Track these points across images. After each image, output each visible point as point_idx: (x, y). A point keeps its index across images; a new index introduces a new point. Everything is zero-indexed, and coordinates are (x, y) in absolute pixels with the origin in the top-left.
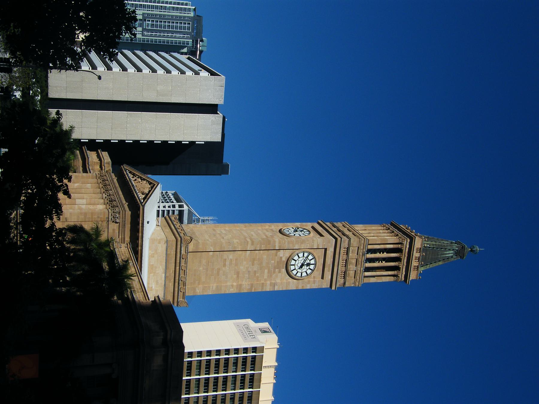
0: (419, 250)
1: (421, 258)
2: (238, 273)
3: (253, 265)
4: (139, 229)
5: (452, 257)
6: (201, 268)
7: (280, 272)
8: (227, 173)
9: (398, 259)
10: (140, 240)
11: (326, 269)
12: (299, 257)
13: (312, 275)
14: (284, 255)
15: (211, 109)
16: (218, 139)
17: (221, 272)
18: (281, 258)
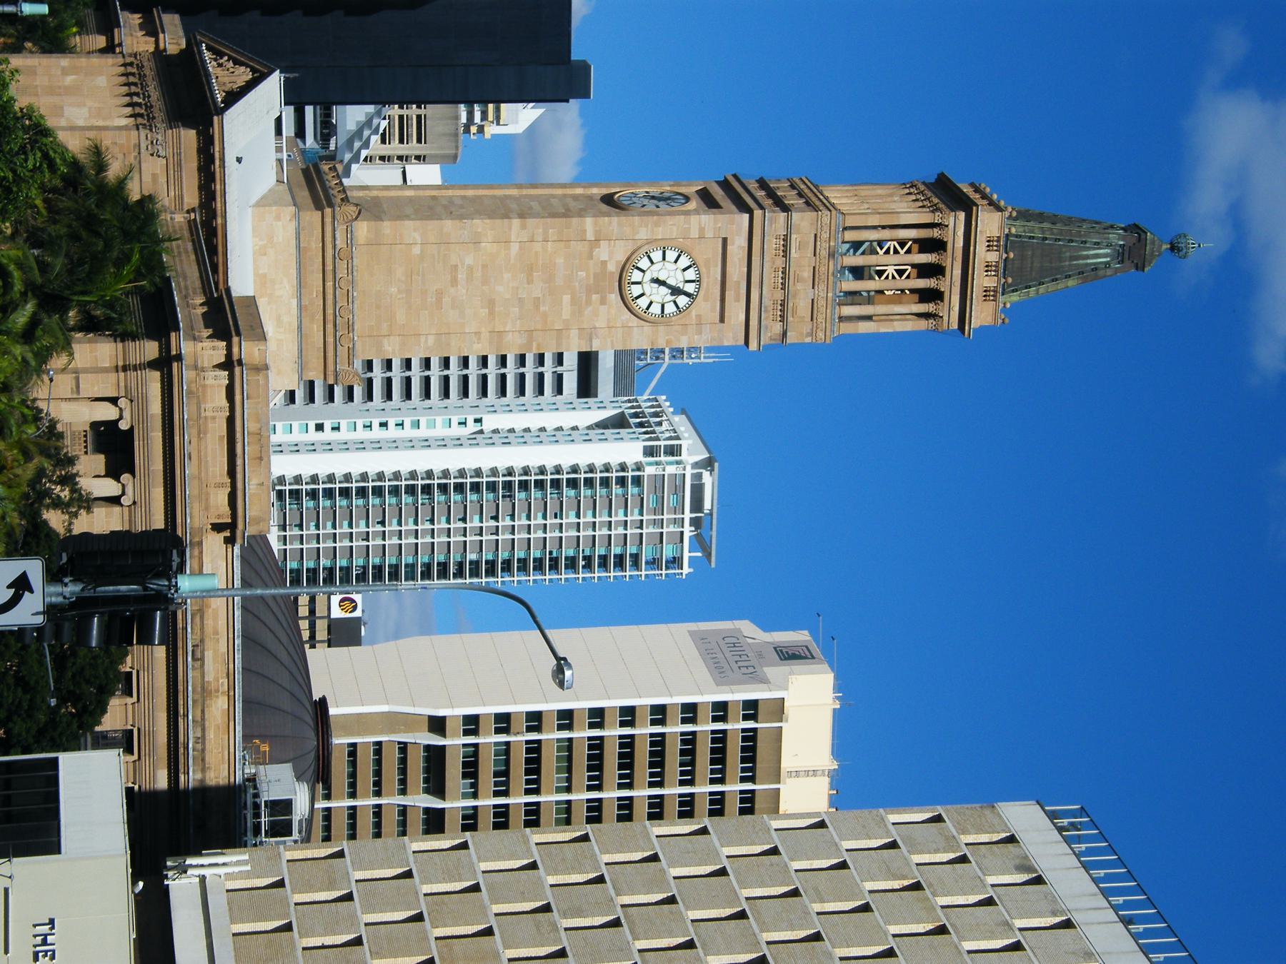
1: (1001, 265)
2: (491, 304)
3: (530, 282)
4: (214, 173)
5: (1107, 265)
6: (394, 290)
7: (603, 301)
8: (586, 94)
9: (934, 271)
10: (218, 199)
11: (729, 295)
12: (652, 262)
13: (694, 312)
17: (446, 300)
18: (604, 263)
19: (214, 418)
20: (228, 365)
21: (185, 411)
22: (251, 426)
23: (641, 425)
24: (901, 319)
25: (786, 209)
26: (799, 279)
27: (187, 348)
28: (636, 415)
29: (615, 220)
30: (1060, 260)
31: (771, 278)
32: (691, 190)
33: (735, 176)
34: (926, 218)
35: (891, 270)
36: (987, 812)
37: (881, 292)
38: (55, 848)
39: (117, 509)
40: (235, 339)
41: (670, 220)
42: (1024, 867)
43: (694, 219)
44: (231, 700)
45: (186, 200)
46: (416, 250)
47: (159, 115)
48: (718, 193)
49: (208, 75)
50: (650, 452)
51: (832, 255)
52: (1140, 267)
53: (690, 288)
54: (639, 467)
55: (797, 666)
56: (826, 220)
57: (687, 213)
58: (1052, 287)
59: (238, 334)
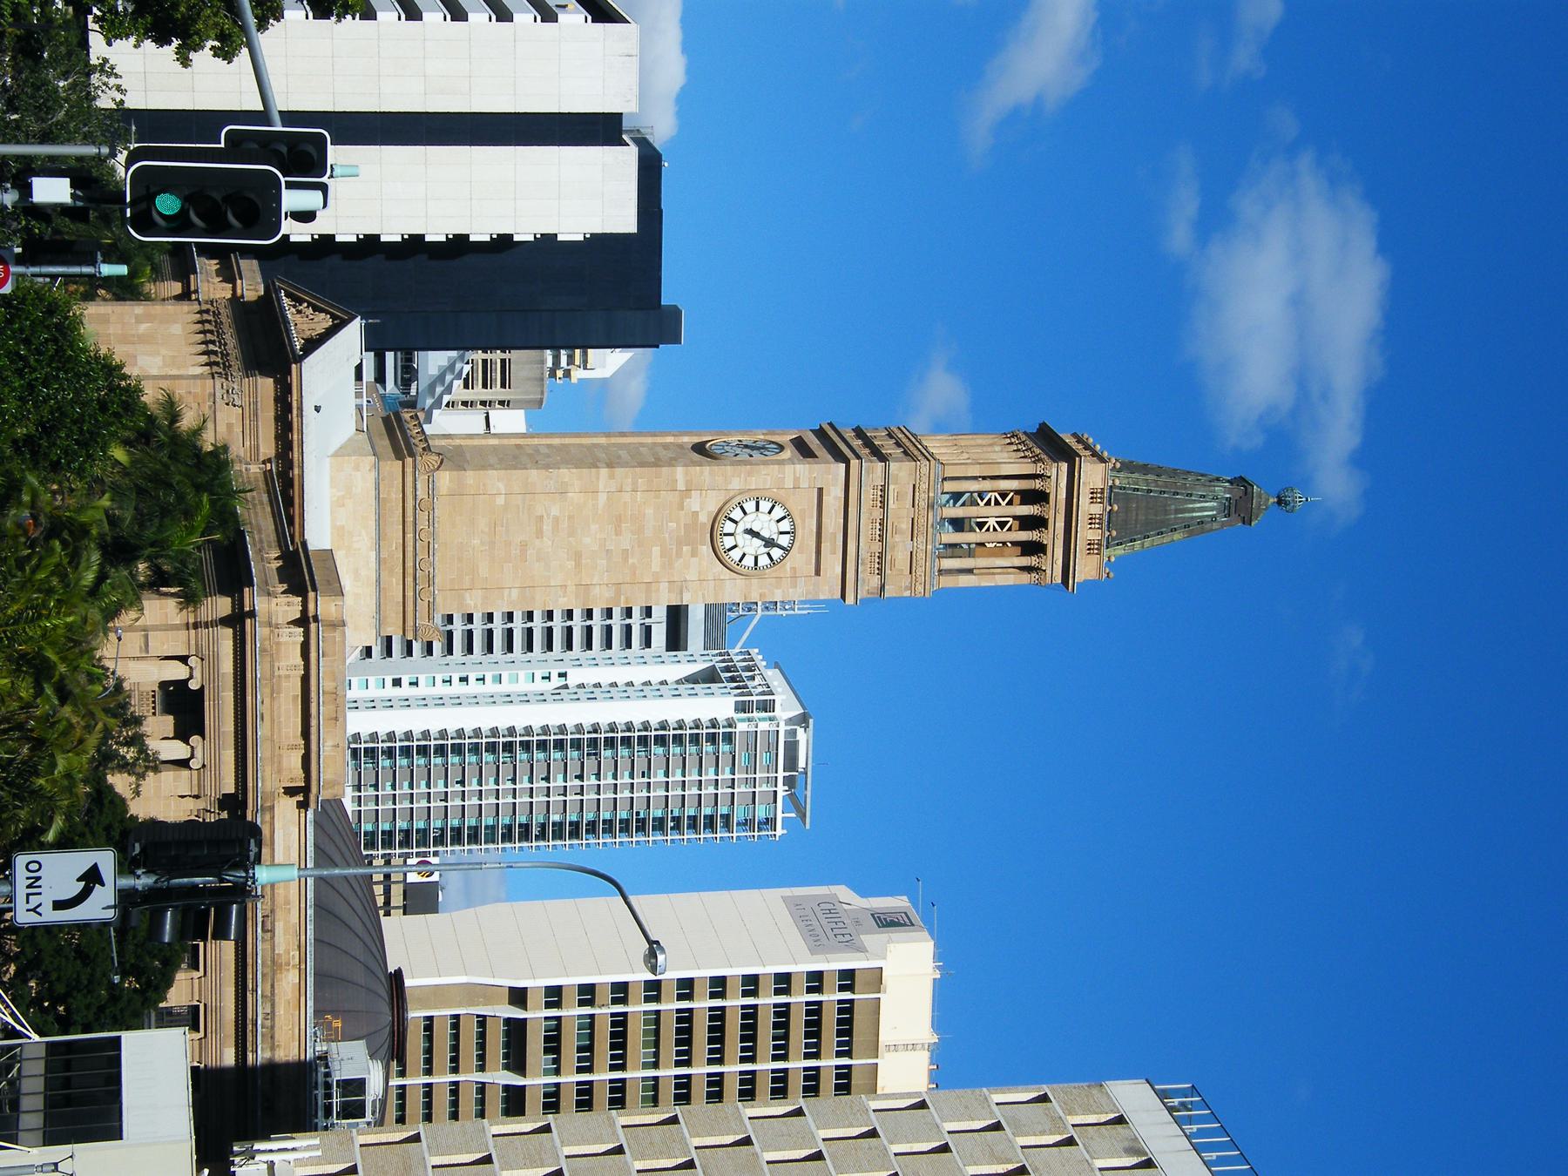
1: (1106, 518)
2: (577, 557)
3: (618, 533)
6: (476, 542)
7: (694, 554)
8: (676, 339)
9: (1038, 523)
13: (788, 563)
14: (703, 506)
15: (598, 129)
16: (626, 222)
18: (696, 514)
19: (288, 677)
20: (303, 621)
21: (258, 669)
22: (327, 684)
23: (732, 679)
24: (1001, 572)
25: (883, 458)
26: (896, 531)
27: (261, 604)
28: (727, 669)
29: (707, 469)
30: (1166, 512)
31: (868, 530)
32: (785, 439)
33: (831, 424)
34: (1028, 469)
35: (992, 522)
36: (1095, 1091)
37: (983, 544)
38: (116, 1134)
39: (185, 773)
40: (311, 595)
41: (764, 469)
42: (1133, 1150)
43: (789, 468)
44: (303, 973)
45: (262, 450)
46: (500, 500)
47: (236, 364)
48: (813, 442)
49: (286, 322)
50: (742, 707)
51: (930, 506)
52: (1247, 521)
53: (784, 540)
54: (730, 723)
55: (896, 934)
56: (925, 470)
57: (781, 463)
58: (1157, 540)
59: (315, 589)
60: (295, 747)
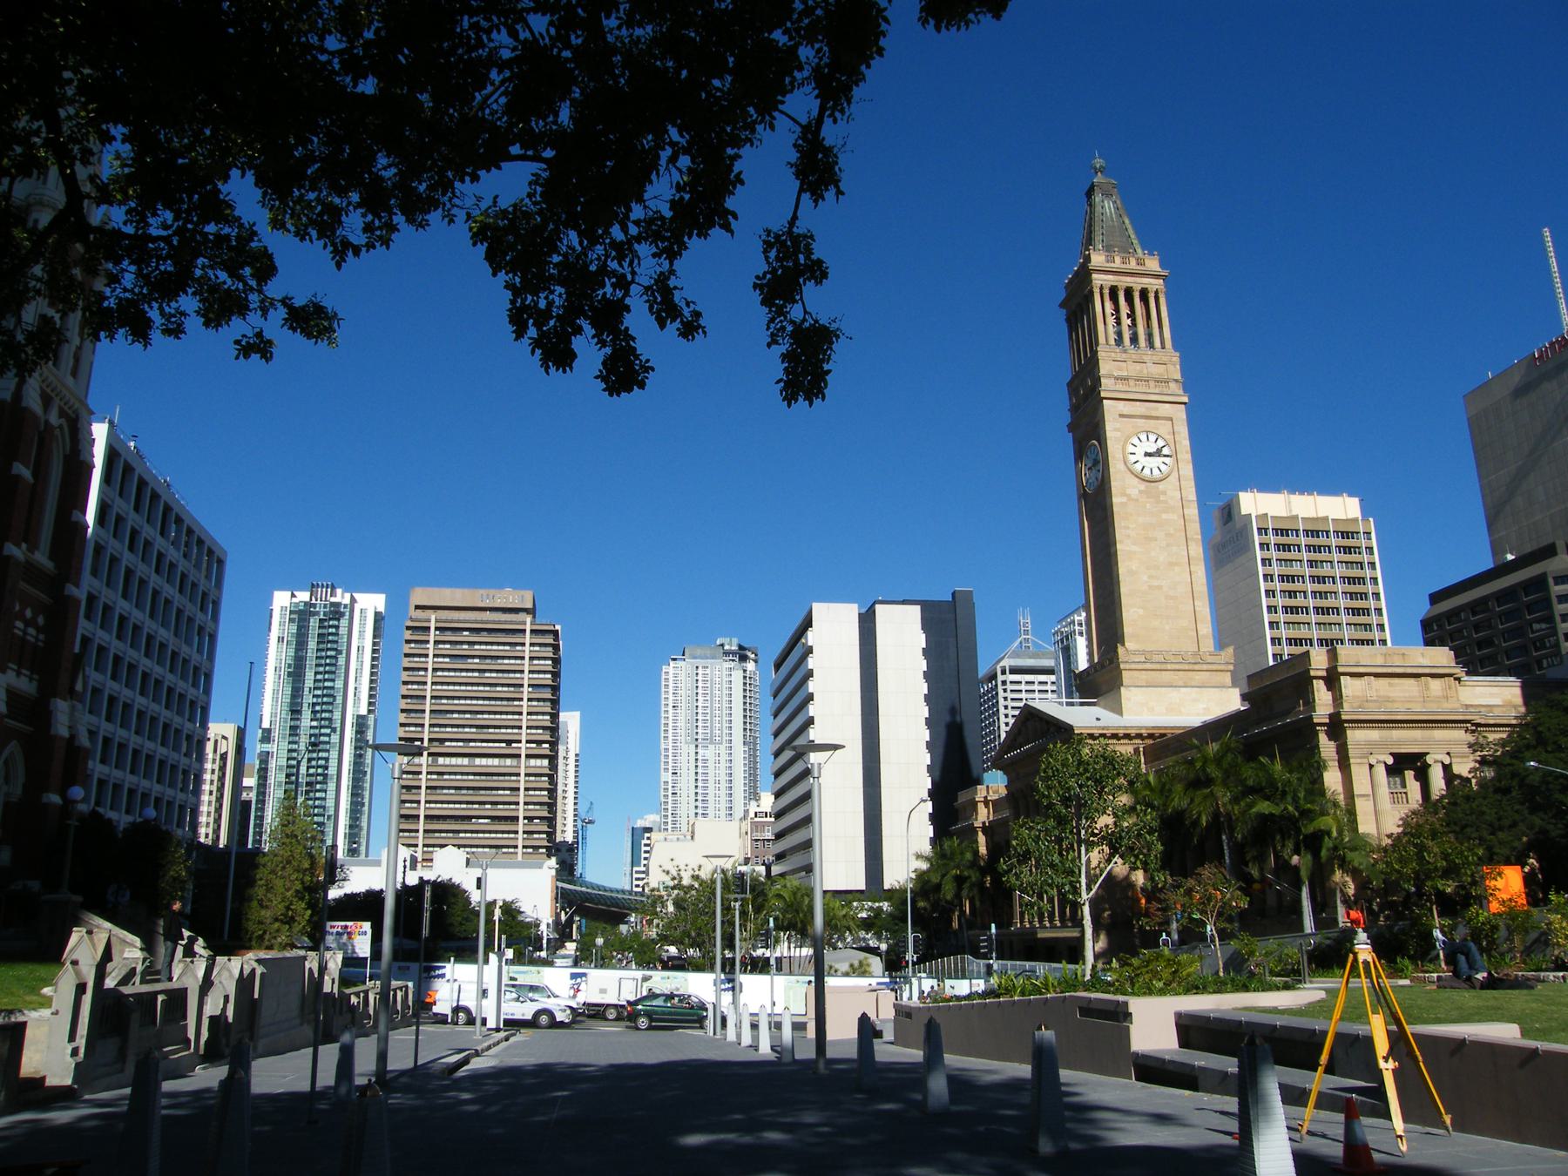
0: (1111, 260)
2: (1171, 564)
7: (1164, 493)
14: (1135, 487)
16: (915, 612)
31: (1142, 387)
46: (1141, 611)
55: (1235, 512)
60: (1426, 684)
